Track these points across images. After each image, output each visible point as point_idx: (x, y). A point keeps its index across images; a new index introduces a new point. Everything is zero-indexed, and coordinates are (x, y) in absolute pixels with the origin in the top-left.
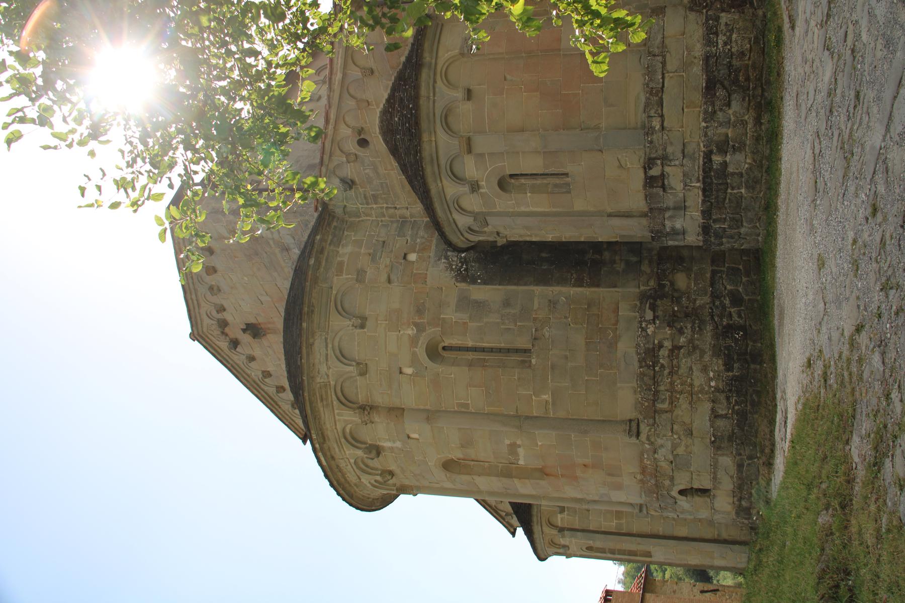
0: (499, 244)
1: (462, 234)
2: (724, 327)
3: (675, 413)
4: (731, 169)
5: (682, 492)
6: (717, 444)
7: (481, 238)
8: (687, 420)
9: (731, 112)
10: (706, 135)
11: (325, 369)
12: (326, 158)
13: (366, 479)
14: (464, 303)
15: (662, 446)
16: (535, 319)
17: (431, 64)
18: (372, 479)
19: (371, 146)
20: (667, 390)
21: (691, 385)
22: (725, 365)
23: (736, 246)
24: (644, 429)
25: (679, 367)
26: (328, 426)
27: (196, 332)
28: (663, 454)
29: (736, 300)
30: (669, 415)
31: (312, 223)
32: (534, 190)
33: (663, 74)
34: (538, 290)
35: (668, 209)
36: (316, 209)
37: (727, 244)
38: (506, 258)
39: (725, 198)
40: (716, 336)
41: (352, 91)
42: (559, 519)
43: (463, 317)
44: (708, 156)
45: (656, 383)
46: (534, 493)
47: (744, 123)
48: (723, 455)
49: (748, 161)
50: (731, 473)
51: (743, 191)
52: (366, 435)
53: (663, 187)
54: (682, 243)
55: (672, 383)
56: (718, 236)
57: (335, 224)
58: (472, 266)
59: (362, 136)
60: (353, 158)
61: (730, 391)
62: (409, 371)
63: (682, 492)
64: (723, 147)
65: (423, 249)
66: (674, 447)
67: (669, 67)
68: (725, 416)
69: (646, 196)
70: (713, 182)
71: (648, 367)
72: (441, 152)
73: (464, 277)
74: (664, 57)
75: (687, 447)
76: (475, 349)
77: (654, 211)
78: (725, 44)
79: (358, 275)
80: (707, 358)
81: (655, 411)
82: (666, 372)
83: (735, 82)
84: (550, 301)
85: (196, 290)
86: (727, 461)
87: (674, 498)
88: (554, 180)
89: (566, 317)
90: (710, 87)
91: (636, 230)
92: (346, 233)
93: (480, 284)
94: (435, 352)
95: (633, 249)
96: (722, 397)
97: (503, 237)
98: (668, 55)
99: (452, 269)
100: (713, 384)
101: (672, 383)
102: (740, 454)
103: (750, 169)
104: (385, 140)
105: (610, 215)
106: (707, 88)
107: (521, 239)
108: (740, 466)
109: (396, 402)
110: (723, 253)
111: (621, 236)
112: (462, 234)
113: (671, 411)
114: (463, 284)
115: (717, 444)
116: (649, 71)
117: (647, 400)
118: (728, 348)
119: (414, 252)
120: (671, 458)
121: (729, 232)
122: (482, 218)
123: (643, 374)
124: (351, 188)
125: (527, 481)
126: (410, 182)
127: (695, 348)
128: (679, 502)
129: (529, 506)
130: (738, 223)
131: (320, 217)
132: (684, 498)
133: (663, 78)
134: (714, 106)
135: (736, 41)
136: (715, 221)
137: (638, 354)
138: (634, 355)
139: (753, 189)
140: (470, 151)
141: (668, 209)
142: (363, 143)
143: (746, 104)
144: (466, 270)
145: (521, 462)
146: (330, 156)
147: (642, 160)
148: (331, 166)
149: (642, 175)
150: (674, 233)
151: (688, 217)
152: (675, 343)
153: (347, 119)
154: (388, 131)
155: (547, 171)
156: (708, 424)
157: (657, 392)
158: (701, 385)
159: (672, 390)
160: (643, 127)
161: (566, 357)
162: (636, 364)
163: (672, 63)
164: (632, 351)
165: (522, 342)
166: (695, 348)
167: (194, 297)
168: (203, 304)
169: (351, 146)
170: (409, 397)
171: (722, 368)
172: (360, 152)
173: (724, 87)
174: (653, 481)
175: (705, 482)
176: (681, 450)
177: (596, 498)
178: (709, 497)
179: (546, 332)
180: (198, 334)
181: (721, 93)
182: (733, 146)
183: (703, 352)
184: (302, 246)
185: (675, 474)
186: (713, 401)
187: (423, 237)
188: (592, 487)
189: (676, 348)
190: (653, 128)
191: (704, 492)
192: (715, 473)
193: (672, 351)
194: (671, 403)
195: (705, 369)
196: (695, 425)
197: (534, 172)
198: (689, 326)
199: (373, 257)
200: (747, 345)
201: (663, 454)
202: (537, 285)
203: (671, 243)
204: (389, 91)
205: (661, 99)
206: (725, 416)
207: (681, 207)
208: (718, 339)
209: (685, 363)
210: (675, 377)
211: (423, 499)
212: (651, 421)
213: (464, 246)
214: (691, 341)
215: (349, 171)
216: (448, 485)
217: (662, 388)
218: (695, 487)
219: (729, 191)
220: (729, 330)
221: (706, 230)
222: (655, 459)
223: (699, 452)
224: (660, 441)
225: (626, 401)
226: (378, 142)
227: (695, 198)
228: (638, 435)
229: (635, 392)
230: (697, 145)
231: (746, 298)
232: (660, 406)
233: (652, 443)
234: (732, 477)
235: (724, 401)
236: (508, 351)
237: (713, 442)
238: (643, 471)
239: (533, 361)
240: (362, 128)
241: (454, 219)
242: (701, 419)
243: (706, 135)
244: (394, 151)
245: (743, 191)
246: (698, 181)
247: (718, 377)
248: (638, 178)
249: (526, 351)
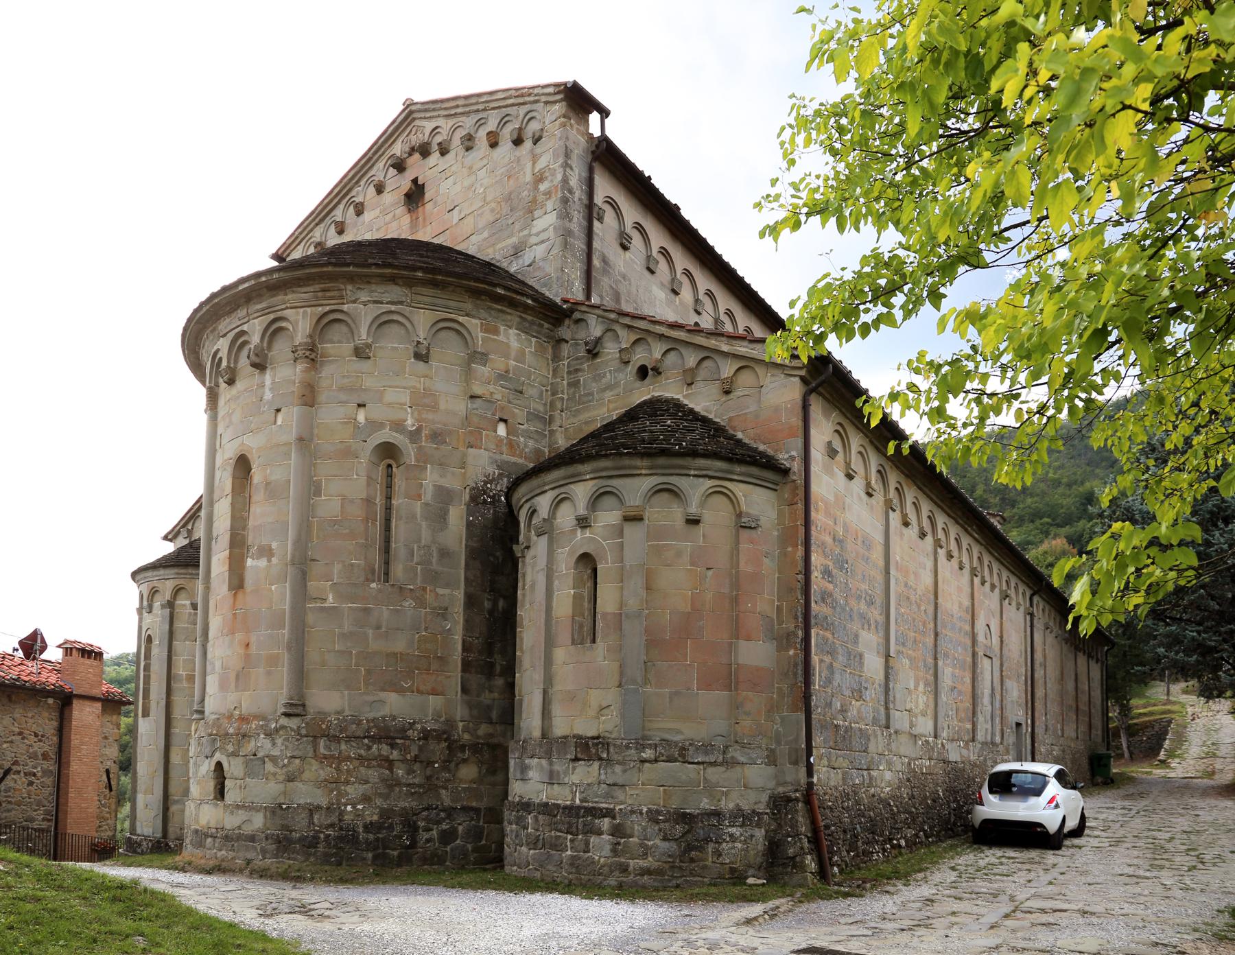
0: (515, 547)
1: (527, 501)
2: (415, 823)
3: (313, 761)
4: (593, 839)
5: (219, 765)
6: (279, 812)
7: (522, 525)
8: (307, 775)
9: (658, 841)
10: (632, 812)
11: (363, 306)
12: (627, 321)
13: (223, 345)
14: (445, 496)
15: (274, 744)
16: (424, 589)
17: (732, 473)
18: (223, 354)
19: (638, 384)
20: (340, 753)
21: (347, 782)
22: (371, 823)
23: (508, 840)
24: (293, 723)
25: (368, 767)
26: (290, 297)
27: (413, 108)
28: (263, 744)
29: (448, 837)
30: (311, 754)
31: (547, 294)
32: (577, 598)
33: (703, 763)
34: (460, 594)
35: (551, 764)
36: (565, 301)
37: (511, 829)
38: (498, 554)
39: (560, 831)
40: (404, 812)
41: (706, 363)
42: (183, 601)
43: (428, 496)
45: (349, 738)
46: (213, 575)
47: (644, 856)
48: (265, 817)
49: (602, 860)
50: (244, 827)
51: (569, 853)
52: (281, 349)
54: (511, 776)
55: (349, 758)
56: (520, 821)
57: (546, 325)
58: (489, 509)
59: (650, 373)
60: (626, 358)
61: (341, 829)
62: (361, 417)
63: (219, 765)
64: (617, 831)
65: (511, 444)
66: (274, 759)
67: (710, 770)
68: (311, 823)
70: (579, 818)
71: (368, 730)
72: (628, 481)
73: (477, 497)
74: (721, 765)
75: (274, 774)
76: (388, 509)
77: (550, 745)
78: (731, 836)
79: (483, 354)
80: (379, 802)
81: (315, 737)
82: (362, 752)
83: (690, 848)
84: (446, 609)
86: (258, 821)
87: (212, 756)
88: (587, 629)
89: (426, 629)
90: (684, 818)
91: (530, 722)
92: (534, 340)
93: (467, 519)
94: (388, 452)
95: (508, 714)
96: (334, 819)
97: (523, 551)
98: (723, 769)
99: (486, 483)
100: (349, 808)
101: (349, 758)
102: (267, 839)
103: (593, 863)
104: (645, 403)
105: (545, 692)
106: (685, 814)
107: (520, 576)
108: (252, 838)
109: (322, 397)
110: (500, 821)
111: (521, 701)
112: (527, 501)
113: (315, 757)
114: (467, 497)
115: (276, 810)
116: (707, 747)
117: (328, 728)
118: (391, 828)
119: (508, 434)
120: (260, 755)
121: (523, 833)
122: (547, 529)
123: (359, 723)
124: (589, 351)
125: (227, 567)
126: (593, 435)
127: (391, 787)
128: (207, 761)
129: (197, 566)
130: (534, 843)
131: (555, 304)
132: (213, 768)
133: (698, 763)
134: (664, 821)
135: (734, 848)
136: (536, 818)
137: (383, 718)
138: (382, 713)
139: (572, 865)
140: (627, 519)
141: (551, 764)
142: (643, 372)
143: (665, 858)
144: (485, 501)
145: (249, 562)
146: (629, 327)
147: (607, 734)
148: (617, 328)
149: (590, 734)
150: (524, 769)
151: (541, 786)
152: (397, 764)
153: (673, 353)
154: (655, 407)
155: (599, 616)
156: (302, 801)
157: (337, 739)
158: (348, 794)
159: (341, 759)
160: (645, 738)
161: (378, 627)
162: (371, 716)
163: (714, 774)
164: (385, 711)
165: (398, 571)
166: (391, 787)
168: (451, 122)
169: (641, 357)
170: (331, 415)
171: (368, 819)
173: (684, 834)
174: (231, 731)
175: (231, 796)
176: (269, 767)
177: (209, 656)
178: (215, 798)
179: (409, 604)
180: (411, 112)
181: (679, 829)
182: (619, 843)
183: (386, 797)
184: (519, 277)
185: (240, 760)
186: (328, 808)
187: (526, 446)
188: (221, 651)
189: (390, 764)
190: (643, 748)
191: (220, 793)
192: (243, 806)
193: (387, 759)
194: (325, 757)
195: (366, 799)
196: (300, 785)
197: (599, 601)
198: (416, 781)
199: (503, 376)
200: (394, 849)
201: (263, 744)
202: (466, 593)
203: (512, 763)
204: (703, 413)
205: (675, 760)
206: (311, 823)
207: (553, 779)
208: (401, 815)
209: (373, 774)
210: (356, 763)
211: (201, 420)
212: (304, 732)
213: (514, 502)
214: (399, 784)
215: (610, 350)
216: (218, 462)
217: (343, 747)
218: (227, 782)
219: (569, 837)
220: (413, 829)
221: (526, 806)
222: (258, 735)
223: (267, 790)
224: (279, 741)
225: (328, 701)
226: (644, 393)
227: (561, 796)
228: (287, 715)
229: (338, 713)
230: (623, 801)
231: (448, 849)
232: (322, 743)
233: (277, 730)
234: (239, 828)
235: (329, 822)
236: (386, 549)
237: (280, 805)
238: (243, 719)
239: (373, 585)
240: (660, 373)
241: (545, 492)
242: (307, 793)
243: (632, 812)
244: (631, 415)
245: (569, 853)
246: (581, 801)
247: (358, 815)
248: (587, 728)
249: (387, 574)
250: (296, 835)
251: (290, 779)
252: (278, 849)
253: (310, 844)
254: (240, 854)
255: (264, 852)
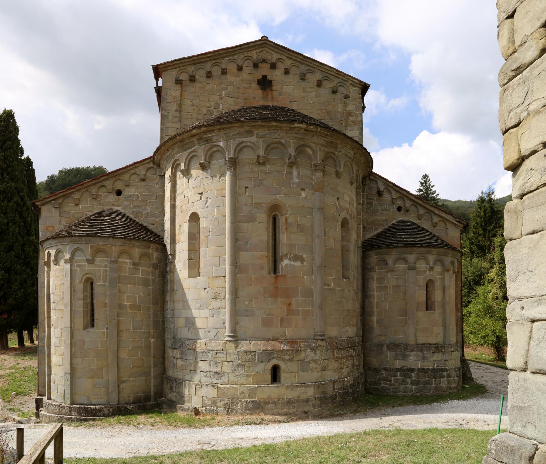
6: (321, 386)
8: (330, 367)
19: (398, 212)
44: (446, 370)
53: (434, 352)
66: (315, 361)
68: (334, 389)
69: (430, 344)
85: (303, 64)
108: (307, 401)
115: (320, 385)
141: (424, 354)
156: (329, 379)
167: (298, 59)
172: (395, 208)
176: (312, 365)
206: (334, 389)
217: (342, 352)
226: (401, 217)
250: (328, 395)
251: (324, 369)
252: (321, 404)
253: (333, 398)
254: (300, 410)
255: (314, 406)
